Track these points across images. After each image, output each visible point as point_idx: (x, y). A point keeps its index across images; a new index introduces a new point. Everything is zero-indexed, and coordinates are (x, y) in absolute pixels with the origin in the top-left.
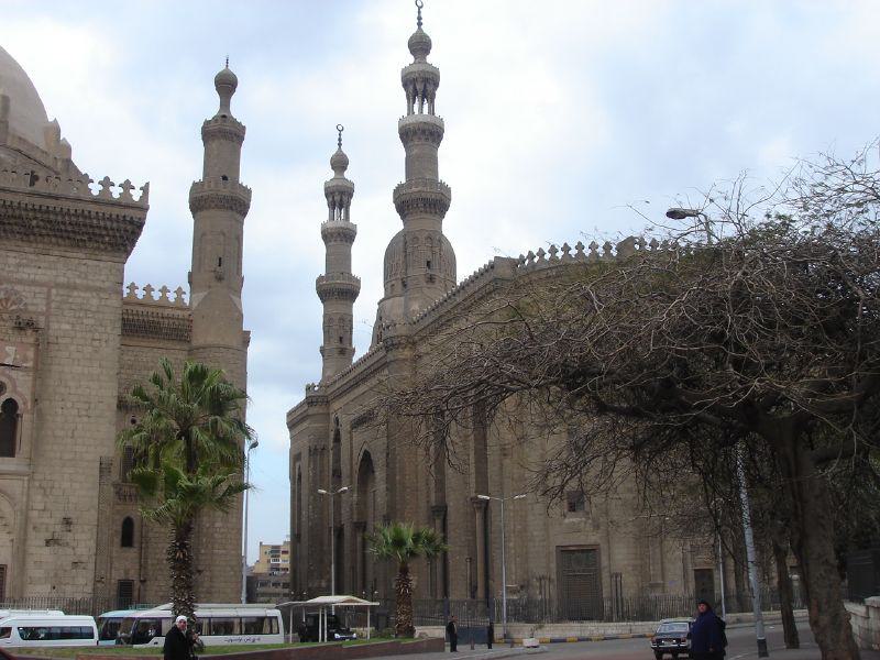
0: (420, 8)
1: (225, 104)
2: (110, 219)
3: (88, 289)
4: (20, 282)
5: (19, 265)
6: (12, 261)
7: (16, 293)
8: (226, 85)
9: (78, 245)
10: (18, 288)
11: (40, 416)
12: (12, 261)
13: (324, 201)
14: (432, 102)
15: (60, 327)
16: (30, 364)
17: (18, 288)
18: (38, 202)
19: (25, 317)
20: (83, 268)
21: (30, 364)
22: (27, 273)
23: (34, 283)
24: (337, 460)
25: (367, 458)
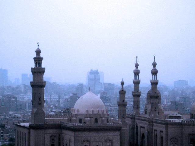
9: (115, 131)
13: (133, 74)
14: (156, 75)
15: (114, 140)
22: (110, 135)
24: (137, 130)
25: (143, 134)
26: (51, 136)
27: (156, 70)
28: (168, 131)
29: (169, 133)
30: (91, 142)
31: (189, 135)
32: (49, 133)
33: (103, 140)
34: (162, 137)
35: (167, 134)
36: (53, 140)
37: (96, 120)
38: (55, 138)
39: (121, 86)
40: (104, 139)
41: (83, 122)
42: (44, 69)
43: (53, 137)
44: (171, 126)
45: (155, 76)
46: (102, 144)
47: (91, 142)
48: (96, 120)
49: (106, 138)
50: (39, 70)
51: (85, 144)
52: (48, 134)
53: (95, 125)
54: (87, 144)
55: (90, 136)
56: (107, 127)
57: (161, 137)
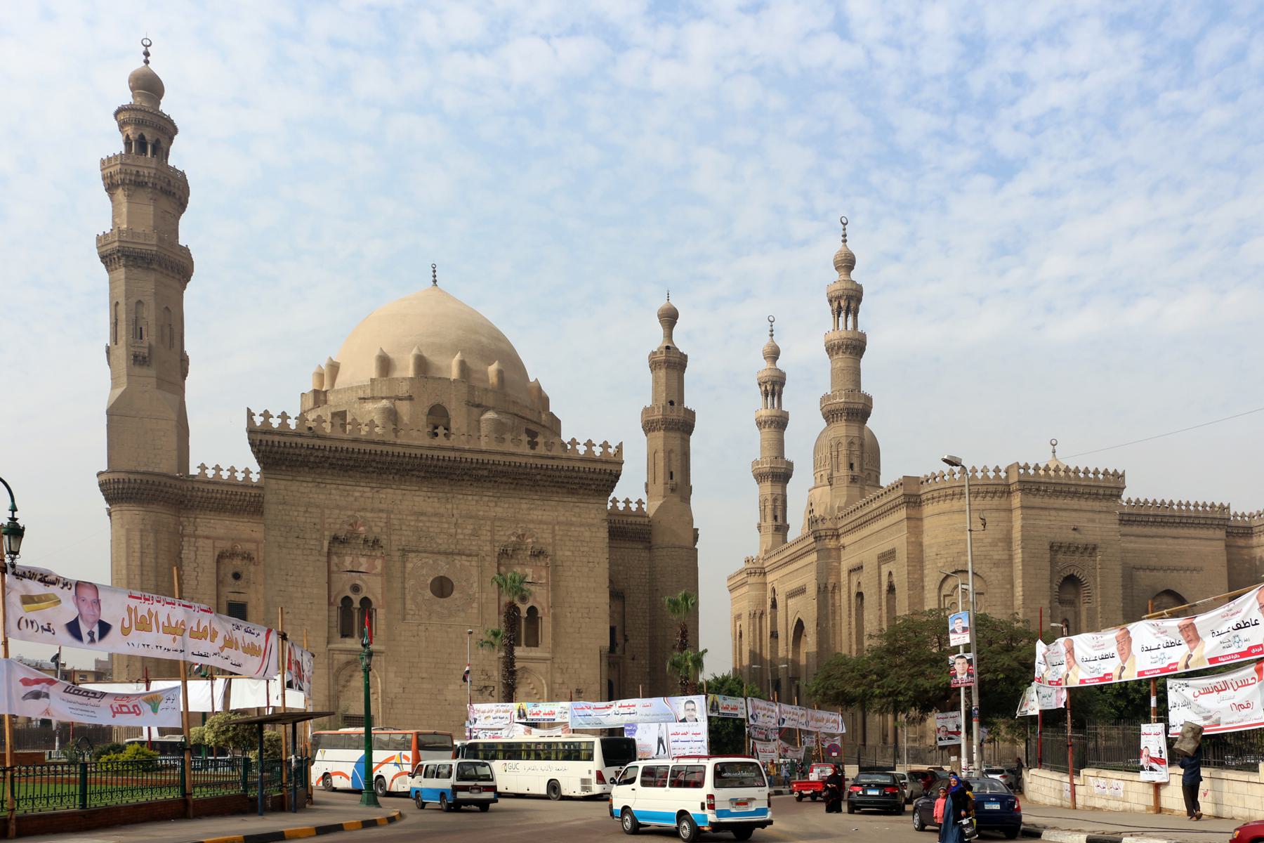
1: (669, 336)
2: (594, 472)
3: (581, 525)
4: (532, 521)
5: (530, 509)
6: (524, 506)
7: (530, 530)
8: (669, 318)
9: (572, 492)
10: (531, 526)
12: (524, 506)
17: (531, 526)
18: (539, 462)
19: (538, 547)
20: (577, 510)
23: (541, 522)
26: (221, 557)
28: (926, 540)
29: (929, 553)
30: (396, 555)
31: (1055, 548)
33: (487, 548)
34: (891, 589)
35: (917, 559)
39: (659, 330)
40: (492, 541)
44: (944, 506)
45: (850, 318)
46: (475, 572)
49: (506, 536)
56: (508, 459)
57: (885, 587)
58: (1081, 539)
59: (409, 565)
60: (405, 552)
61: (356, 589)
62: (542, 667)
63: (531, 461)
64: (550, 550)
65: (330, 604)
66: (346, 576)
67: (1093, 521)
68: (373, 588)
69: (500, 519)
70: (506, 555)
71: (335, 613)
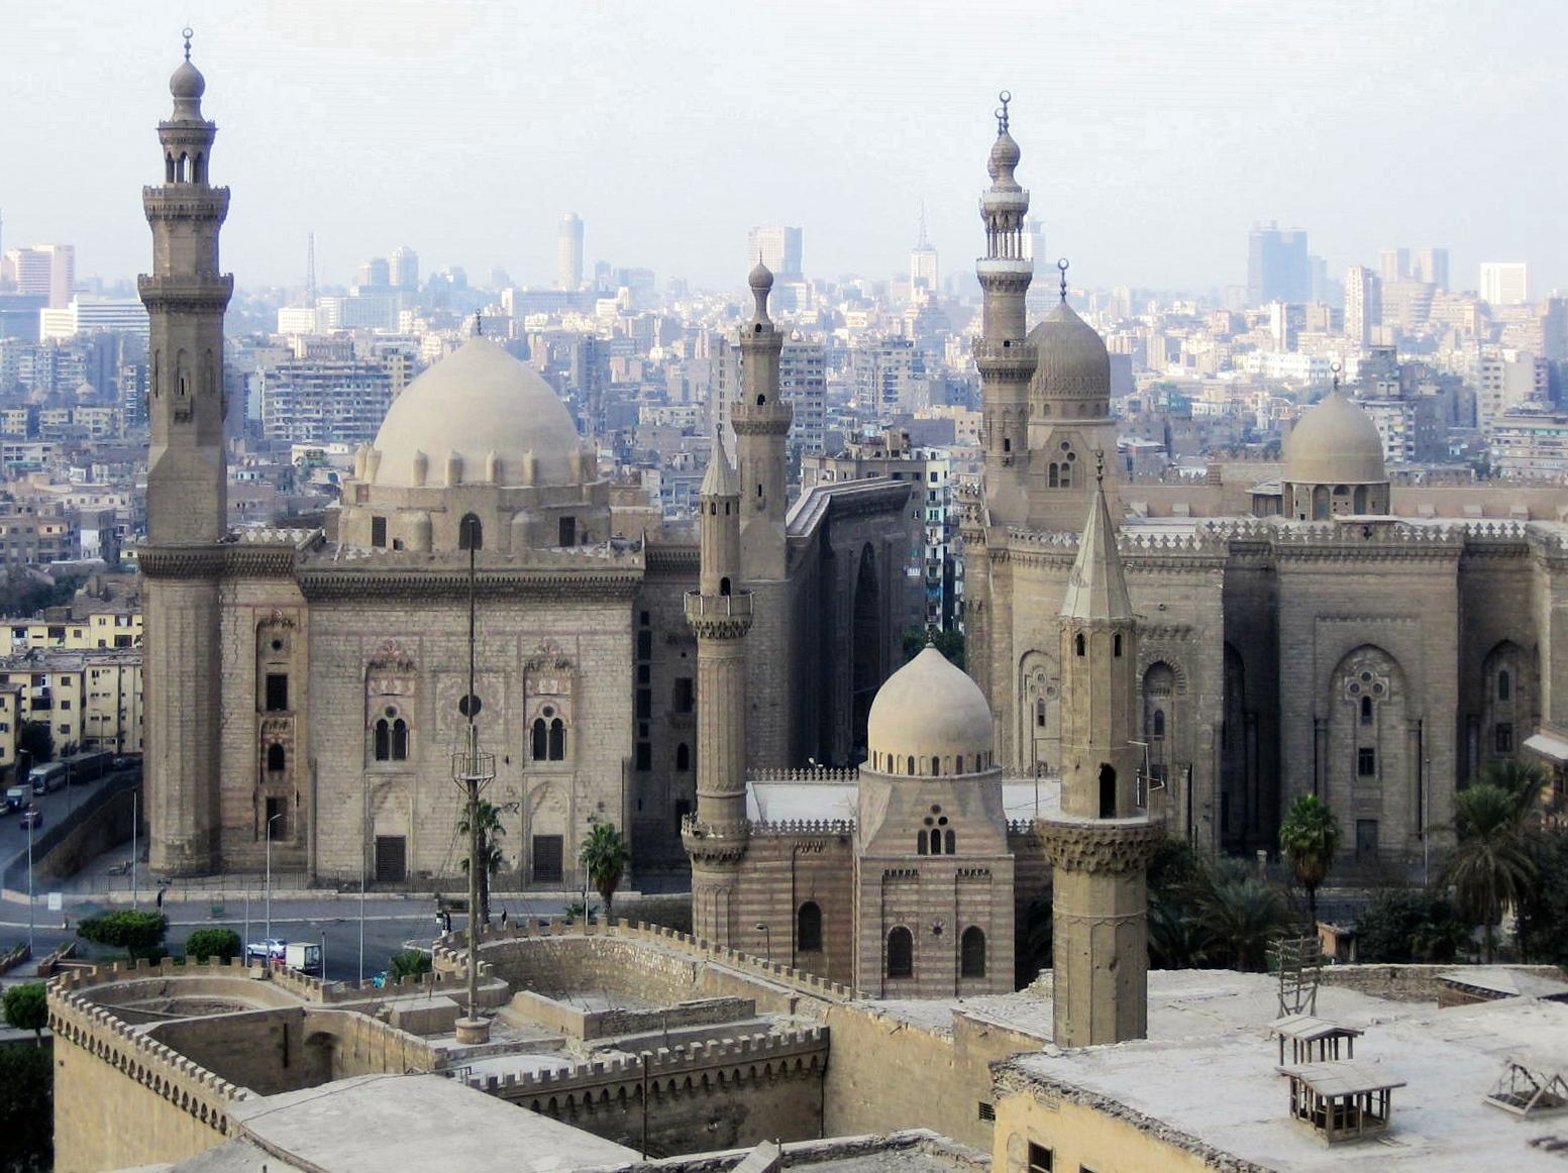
0: (1005, 102)
3: (605, 633)
4: (557, 633)
5: (555, 621)
9: (596, 600)
11: (578, 731)
12: (550, 618)
15: (587, 664)
16: (568, 692)
18: (563, 575)
21: (568, 692)
22: (562, 626)
26: (260, 627)
27: (1018, 189)
30: (427, 676)
32: (247, 605)
33: (514, 663)
36: (277, 645)
37: (471, 532)
38: (293, 636)
39: (752, 300)
40: (519, 657)
41: (390, 544)
42: (224, 194)
43: (278, 629)
46: (501, 689)
47: (427, 676)
48: (471, 532)
49: (531, 649)
50: (178, 204)
51: (384, 683)
52: (241, 611)
53: (449, 558)
54: (397, 683)
55: (421, 634)
56: (532, 575)
58: (1170, 620)
59: (440, 686)
60: (435, 673)
61: (391, 712)
62: (567, 781)
63: (555, 575)
64: (574, 662)
65: (366, 728)
66: (381, 700)
67: (1187, 597)
68: (407, 710)
69: (527, 633)
70: (532, 667)
71: (371, 736)
